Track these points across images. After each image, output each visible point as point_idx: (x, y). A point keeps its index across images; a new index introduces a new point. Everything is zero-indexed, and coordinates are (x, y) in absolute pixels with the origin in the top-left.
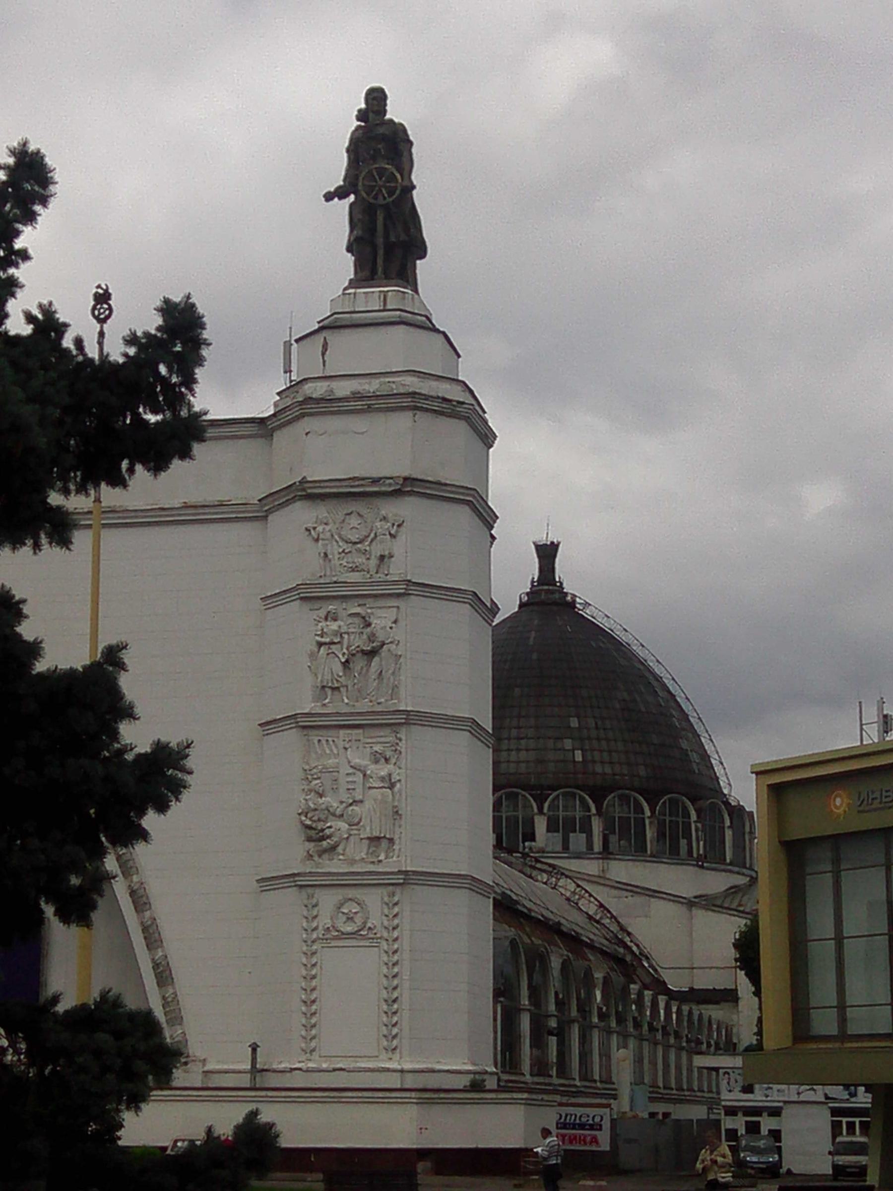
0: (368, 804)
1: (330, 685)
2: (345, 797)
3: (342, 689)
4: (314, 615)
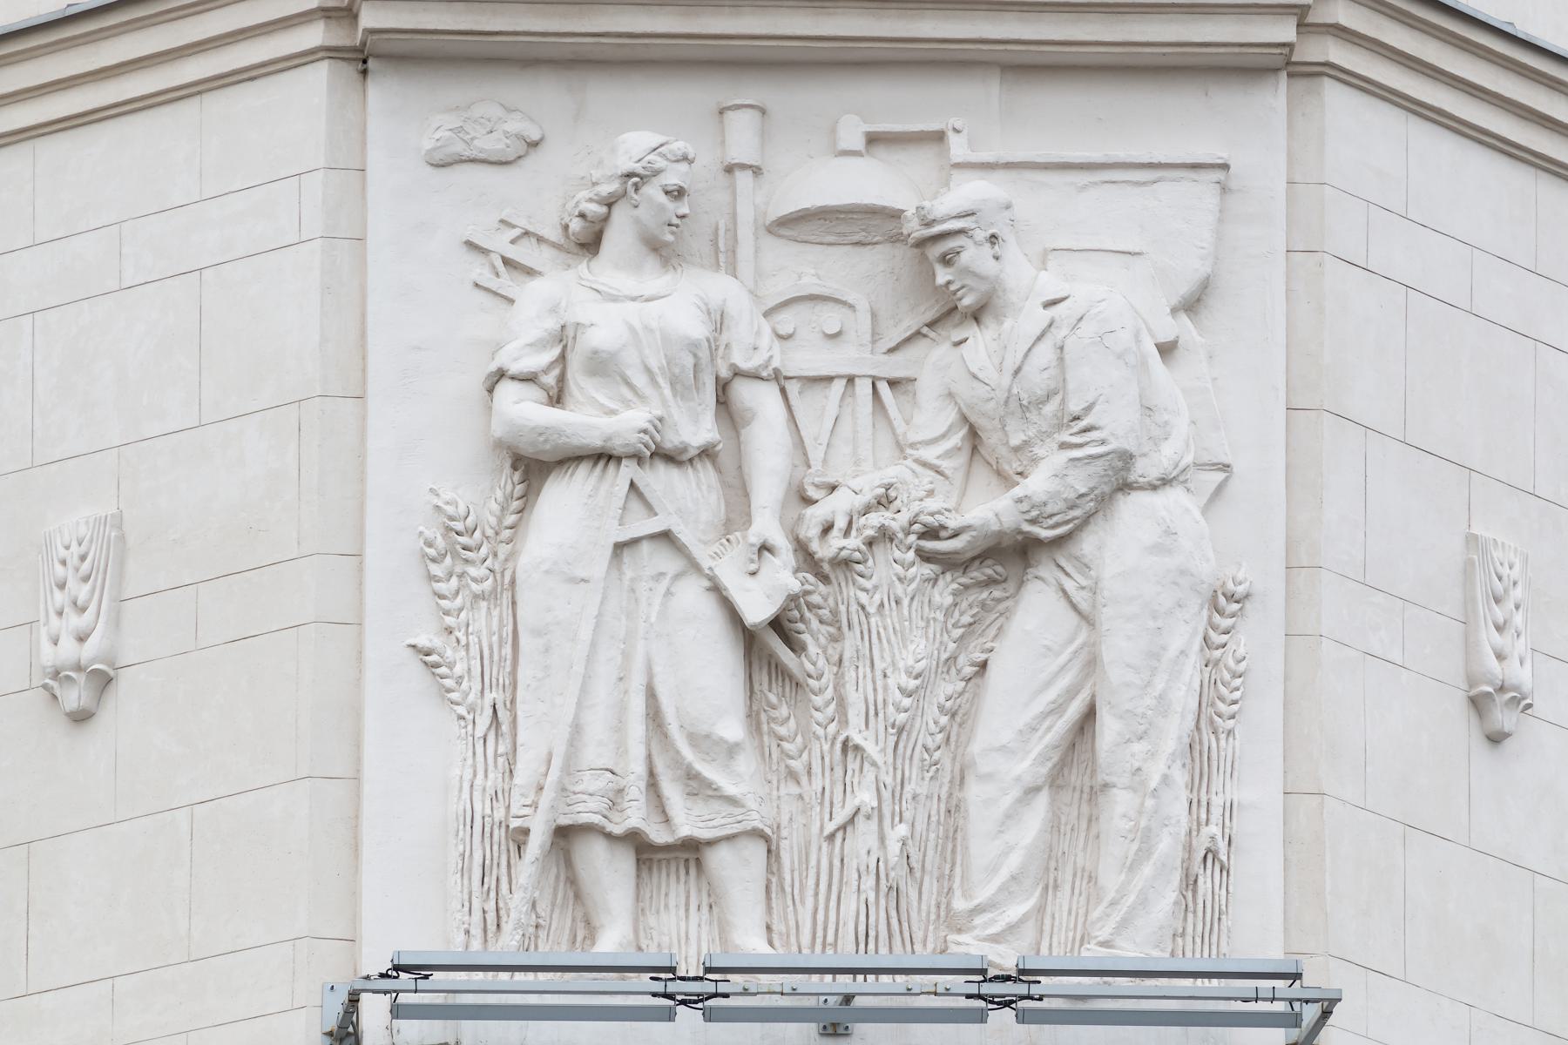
1: (635, 816)
3: (720, 860)
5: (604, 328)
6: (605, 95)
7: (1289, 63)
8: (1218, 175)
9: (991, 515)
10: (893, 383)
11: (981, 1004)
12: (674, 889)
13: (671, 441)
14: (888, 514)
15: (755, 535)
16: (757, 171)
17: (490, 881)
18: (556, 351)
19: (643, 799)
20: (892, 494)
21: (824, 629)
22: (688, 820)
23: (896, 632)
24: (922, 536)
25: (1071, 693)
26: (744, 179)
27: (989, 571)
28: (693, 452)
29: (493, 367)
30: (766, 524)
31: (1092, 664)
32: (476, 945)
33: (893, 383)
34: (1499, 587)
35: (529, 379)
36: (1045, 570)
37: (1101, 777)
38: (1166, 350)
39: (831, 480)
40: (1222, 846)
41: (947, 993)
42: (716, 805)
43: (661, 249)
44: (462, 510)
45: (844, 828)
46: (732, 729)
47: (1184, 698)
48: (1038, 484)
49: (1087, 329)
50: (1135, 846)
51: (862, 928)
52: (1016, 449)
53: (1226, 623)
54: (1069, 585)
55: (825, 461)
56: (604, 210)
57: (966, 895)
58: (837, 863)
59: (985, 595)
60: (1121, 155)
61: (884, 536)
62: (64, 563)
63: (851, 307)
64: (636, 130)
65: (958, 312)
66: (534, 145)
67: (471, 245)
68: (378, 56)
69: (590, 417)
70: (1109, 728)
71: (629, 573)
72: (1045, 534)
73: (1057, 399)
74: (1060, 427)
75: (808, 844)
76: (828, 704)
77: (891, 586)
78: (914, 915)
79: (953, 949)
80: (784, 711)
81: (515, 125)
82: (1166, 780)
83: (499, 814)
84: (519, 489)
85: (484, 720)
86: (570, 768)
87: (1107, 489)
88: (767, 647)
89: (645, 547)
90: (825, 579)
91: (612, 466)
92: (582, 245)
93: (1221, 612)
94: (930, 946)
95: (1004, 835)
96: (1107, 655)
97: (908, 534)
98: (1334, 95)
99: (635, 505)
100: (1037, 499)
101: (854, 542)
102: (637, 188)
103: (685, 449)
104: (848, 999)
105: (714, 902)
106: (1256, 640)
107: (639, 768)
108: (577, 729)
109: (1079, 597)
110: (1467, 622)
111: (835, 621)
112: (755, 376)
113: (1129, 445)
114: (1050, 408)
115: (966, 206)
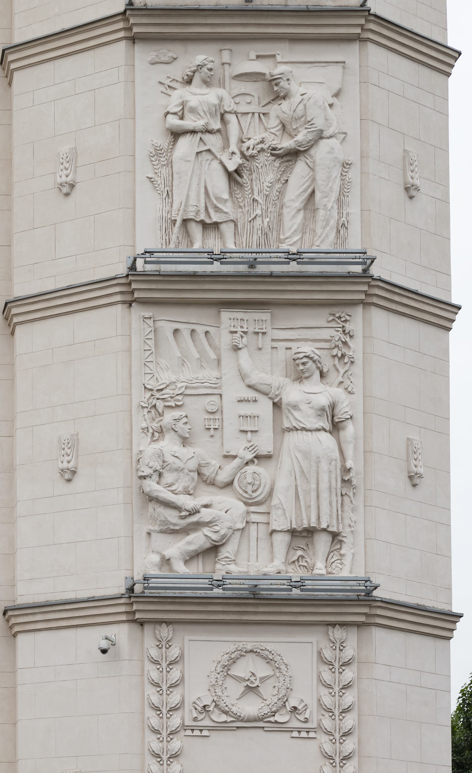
0: (286, 462)
1: (202, 216)
2: (239, 447)
3: (223, 227)
4: (163, 73)
5: (193, 102)
6: (192, 47)
7: (359, 38)
8: (343, 64)
9: (288, 145)
10: (264, 114)
11: (288, 260)
12: (212, 234)
13: (210, 128)
14: (263, 145)
15: (231, 150)
16: (229, 64)
17: (167, 232)
18: (181, 107)
19: (204, 212)
20: (264, 140)
21: (248, 172)
22: (215, 218)
23: (266, 174)
24: (272, 150)
25: (309, 187)
26: (226, 66)
27: (288, 158)
28: (215, 131)
29: (166, 111)
30: (233, 147)
31: (314, 180)
32: (164, 247)
33: (264, 114)
34: (412, 162)
35: (175, 114)
36: (302, 158)
37: (316, 207)
38: (331, 106)
39: (249, 137)
40: (346, 223)
41: (280, 257)
42: (222, 214)
43: (207, 83)
44: (159, 145)
45: (253, 219)
46: (226, 196)
47: (336, 188)
48: (300, 137)
49: (311, 100)
50: (325, 223)
51: (258, 243)
52: (294, 129)
53: (346, 170)
54: (308, 161)
55: (247, 133)
56: (193, 74)
57: (283, 235)
58: (252, 227)
59: (287, 164)
60: (319, 60)
61: (262, 150)
62: (62, 159)
63: (253, 96)
64: (200, 56)
65: (279, 97)
66: (175, 59)
67: (160, 83)
68: (137, 39)
69: (190, 122)
70: (318, 195)
71: (200, 159)
72: (302, 149)
73: (305, 117)
74: (305, 124)
75: (245, 223)
76: (249, 190)
77: (264, 162)
78: (271, 239)
79: (280, 247)
80: (238, 192)
81: (171, 54)
82: (332, 207)
83: (169, 216)
84: (173, 140)
85: (165, 194)
86: (186, 205)
87: (317, 138)
88: (234, 177)
89: (204, 153)
90: (248, 160)
91: (195, 134)
92: (187, 82)
93: (345, 168)
94: (275, 247)
95: (292, 221)
96: (317, 178)
97: (268, 149)
98: (371, 47)
99: (201, 143)
100: (300, 140)
101: (255, 151)
102: (201, 68)
103: (213, 130)
104: (255, 259)
105: (222, 237)
106: (354, 174)
107: (203, 205)
108: (188, 196)
109: (311, 164)
110: (404, 170)
111: (250, 170)
112: (230, 112)
113: (322, 128)
114: (303, 119)
115: (281, 72)
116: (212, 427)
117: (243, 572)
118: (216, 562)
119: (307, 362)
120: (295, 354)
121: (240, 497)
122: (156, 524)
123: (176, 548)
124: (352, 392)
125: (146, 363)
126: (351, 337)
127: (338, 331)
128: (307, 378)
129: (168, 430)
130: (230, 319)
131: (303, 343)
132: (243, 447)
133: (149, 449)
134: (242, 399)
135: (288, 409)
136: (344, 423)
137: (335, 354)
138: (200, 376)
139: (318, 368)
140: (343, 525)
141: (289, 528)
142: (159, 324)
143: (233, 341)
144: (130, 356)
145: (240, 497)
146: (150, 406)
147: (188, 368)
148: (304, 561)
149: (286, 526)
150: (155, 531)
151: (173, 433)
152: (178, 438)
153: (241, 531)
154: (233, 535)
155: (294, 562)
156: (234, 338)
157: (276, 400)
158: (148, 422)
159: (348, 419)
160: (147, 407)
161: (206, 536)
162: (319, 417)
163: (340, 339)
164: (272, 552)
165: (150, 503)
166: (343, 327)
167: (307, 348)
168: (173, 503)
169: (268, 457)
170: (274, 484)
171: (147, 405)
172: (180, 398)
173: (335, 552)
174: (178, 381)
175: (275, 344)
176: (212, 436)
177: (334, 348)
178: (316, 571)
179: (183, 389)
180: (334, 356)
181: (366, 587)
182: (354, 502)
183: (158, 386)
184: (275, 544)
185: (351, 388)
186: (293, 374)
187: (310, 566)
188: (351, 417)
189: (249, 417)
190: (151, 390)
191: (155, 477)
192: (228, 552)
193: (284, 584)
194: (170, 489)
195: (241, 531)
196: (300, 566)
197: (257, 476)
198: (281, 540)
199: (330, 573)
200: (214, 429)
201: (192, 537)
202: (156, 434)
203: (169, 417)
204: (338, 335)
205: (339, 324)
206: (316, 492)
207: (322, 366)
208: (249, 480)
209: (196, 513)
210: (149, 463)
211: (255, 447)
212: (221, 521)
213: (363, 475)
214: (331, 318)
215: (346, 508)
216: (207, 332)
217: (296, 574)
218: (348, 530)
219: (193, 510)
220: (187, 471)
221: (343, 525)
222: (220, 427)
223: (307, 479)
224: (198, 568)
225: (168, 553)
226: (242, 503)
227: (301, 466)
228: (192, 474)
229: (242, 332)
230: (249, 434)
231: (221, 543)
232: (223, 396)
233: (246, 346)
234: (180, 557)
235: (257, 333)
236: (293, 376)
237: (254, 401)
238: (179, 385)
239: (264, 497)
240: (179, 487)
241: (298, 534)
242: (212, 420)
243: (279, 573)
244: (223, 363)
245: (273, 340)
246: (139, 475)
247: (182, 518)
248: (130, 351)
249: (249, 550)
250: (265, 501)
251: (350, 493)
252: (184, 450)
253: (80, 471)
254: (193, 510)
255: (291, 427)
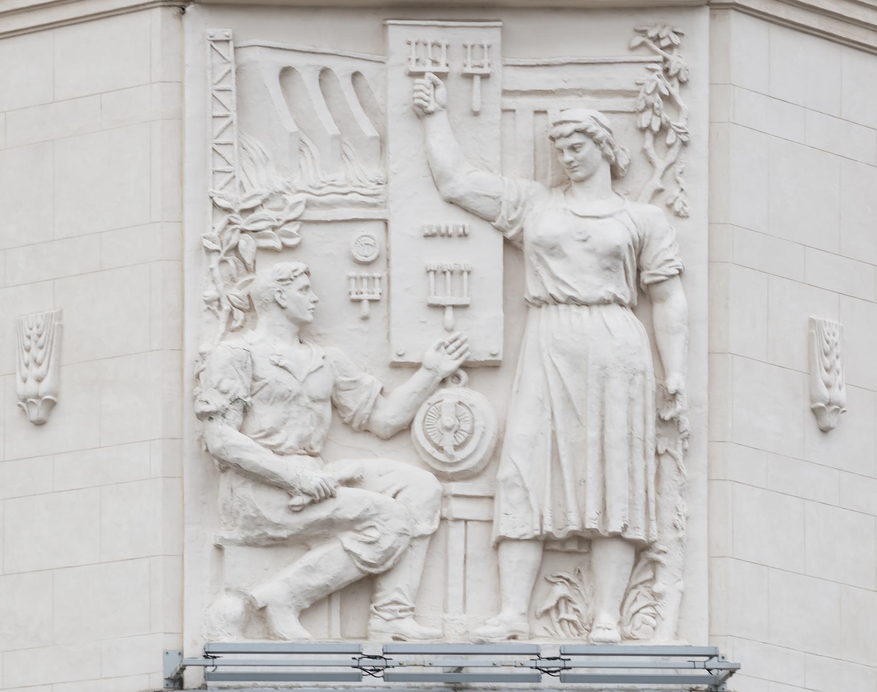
0: (531, 377)
2: (428, 344)
116: (365, 296)
117: (432, 637)
118: (370, 614)
119: (581, 145)
120: (555, 124)
121: (426, 460)
122: (235, 525)
123: (280, 581)
124: (682, 213)
125: (217, 148)
126: (682, 83)
127: (653, 71)
128: (581, 181)
129: (265, 304)
130: (409, 43)
131: (573, 98)
132: (435, 344)
133: (220, 348)
134: (434, 231)
135: (538, 255)
136: (664, 285)
137: (645, 125)
138: (340, 176)
139: (606, 157)
140: (660, 524)
141: (538, 533)
142: (248, 55)
143: (416, 95)
144: (181, 130)
145: (426, 460)
146: (226, 248)
147: (313, 158)
148: (570, 610)
149: (531, 530)
150: (232, 542)
151: (276, 311)
152: (288, 324)
153: (427, 541)
154: (410, 551)
155: (547, 612)
156: (416, 87)
157: (510, 234)
158: (221, 286)
159: (672, 276)
160: (218, 251)
161: (348, 552)
162: (607, 273)
163: (657, 89)
164: (498, 589)
165: (222, 475)
166: (666, 60)
167: (582, 112)
168: (274, 475)
169: (493, 366)
170: (505, 430)
171: (218, 247)
172: (293, 228)
173: (641, 589)
174: (288, 189)
175: (510, 102)
176: (365, 318)
177: (642, 112)
178: (598, 634)
179: (300, 209)
180: (643, 130)
181: (709, 670)
182: (684, 471)
183: (244, 201)
184: (506, 569)
185: (681, 205)
186: (550, 172)
187: (585, 621)
188: (680, 273)
189: (448, 274)
190: (228, 210)
191: (235, 415)
192: (399, 590)
193: (522, 665)
194: (268, 442)
195: (427, 541)
196: (560, 621)
197: (465, 410)
198: (520, 561)
199: (629, 638)
200: (371, 301)
201: (318, 554)
202: (239, 315)
203: (269, 271)
204: (654, 80)
205: (655, 53)
206: (597, 449)
207: (616, 154)
208: (448, 420)
209: (326, 498)
210: (220, 382)
211: (463, 343)
212: (383, 516)
213: (706, 408)
214: (638, 40)
215: (666, 484)
216: (356, 75)
217: (550, 640)
218: (671, 535)
219: (319, 491)
220: (307, 400)
221: (660, 524)
222: (385, 297)
223: (578, 418)
224: (329, 627)
225: (261, 593)
226: (431, 476)
227: (564, 388)
228: (318, 407)
229: (435, 73)
230: (449, 312)
231: (381, 569)
232: (391, 225)
233: (444, 107)
234: (290, 603)
235: (470, 77)
236: (549, 178)
237: (460, 236)
238: (292, 199)
239: (481, 461)
240: (288, 437)
241: (556, 547)
242: (365, 281)
243: (514, 637)
244: (392, 146)
245: (506, 93)
246: (198, 411)
247: (295, 510)
248: (181, 118)
249: (446, 585)
250: (485, 469)
251: (676, 448)
252: (302, 352)
253: (65, 403)
254: (319, 491)
255: (544, 296)
